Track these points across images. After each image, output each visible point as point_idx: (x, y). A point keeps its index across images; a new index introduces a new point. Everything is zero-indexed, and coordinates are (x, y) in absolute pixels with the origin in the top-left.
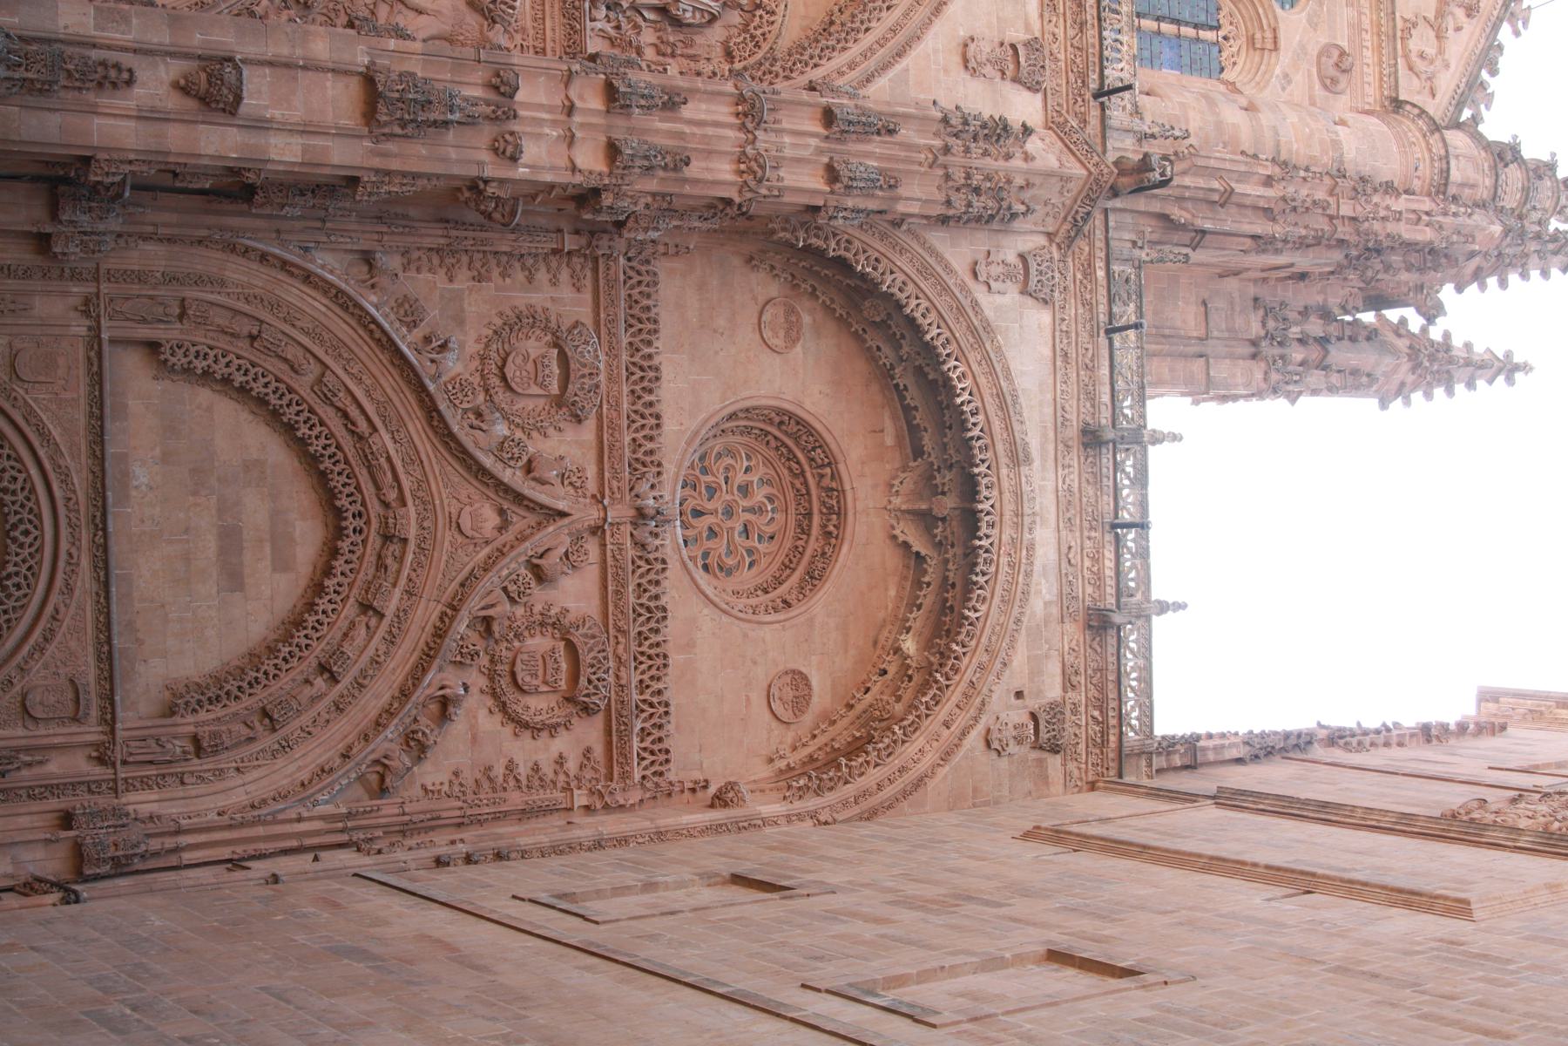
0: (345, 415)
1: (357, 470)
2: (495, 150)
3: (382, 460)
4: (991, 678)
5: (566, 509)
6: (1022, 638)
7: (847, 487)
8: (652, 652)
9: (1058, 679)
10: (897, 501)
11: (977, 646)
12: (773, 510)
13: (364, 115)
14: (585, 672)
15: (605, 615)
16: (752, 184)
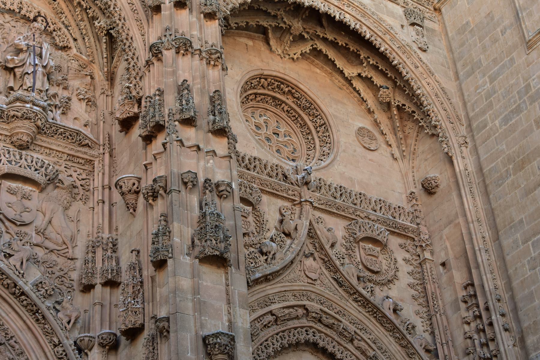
0: (265, 326)
1: (289, 327)
2: (225, 198)
3: (287, 311)
4: (397, 36)
5: (309, 221)
6: (381, 15)
7: (274, 74)
8: (359, 200)
9: (394, 5)
10: (280, 52)
11: (382, 38)
12: (265, 115)
13: (219, 267)
14: (374, 235)
15: (345, 217)
16: (220, 60)
